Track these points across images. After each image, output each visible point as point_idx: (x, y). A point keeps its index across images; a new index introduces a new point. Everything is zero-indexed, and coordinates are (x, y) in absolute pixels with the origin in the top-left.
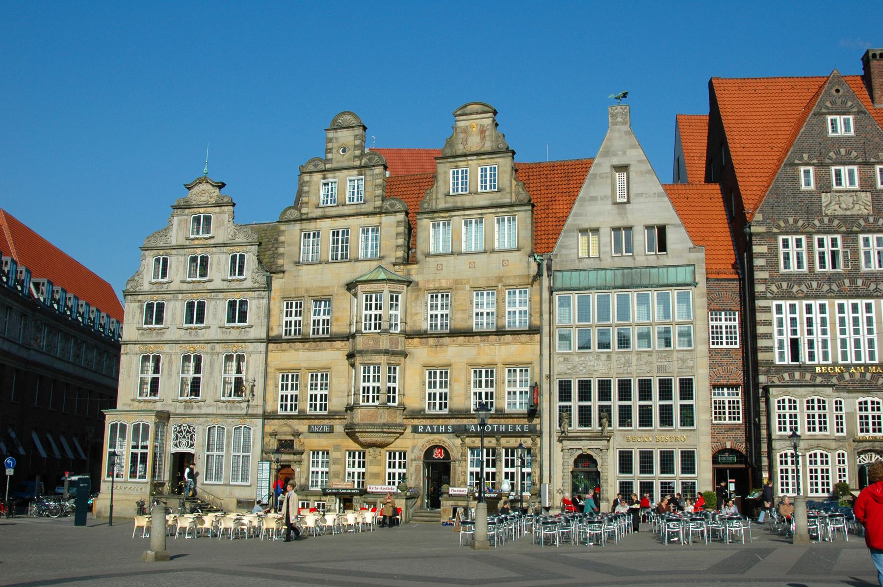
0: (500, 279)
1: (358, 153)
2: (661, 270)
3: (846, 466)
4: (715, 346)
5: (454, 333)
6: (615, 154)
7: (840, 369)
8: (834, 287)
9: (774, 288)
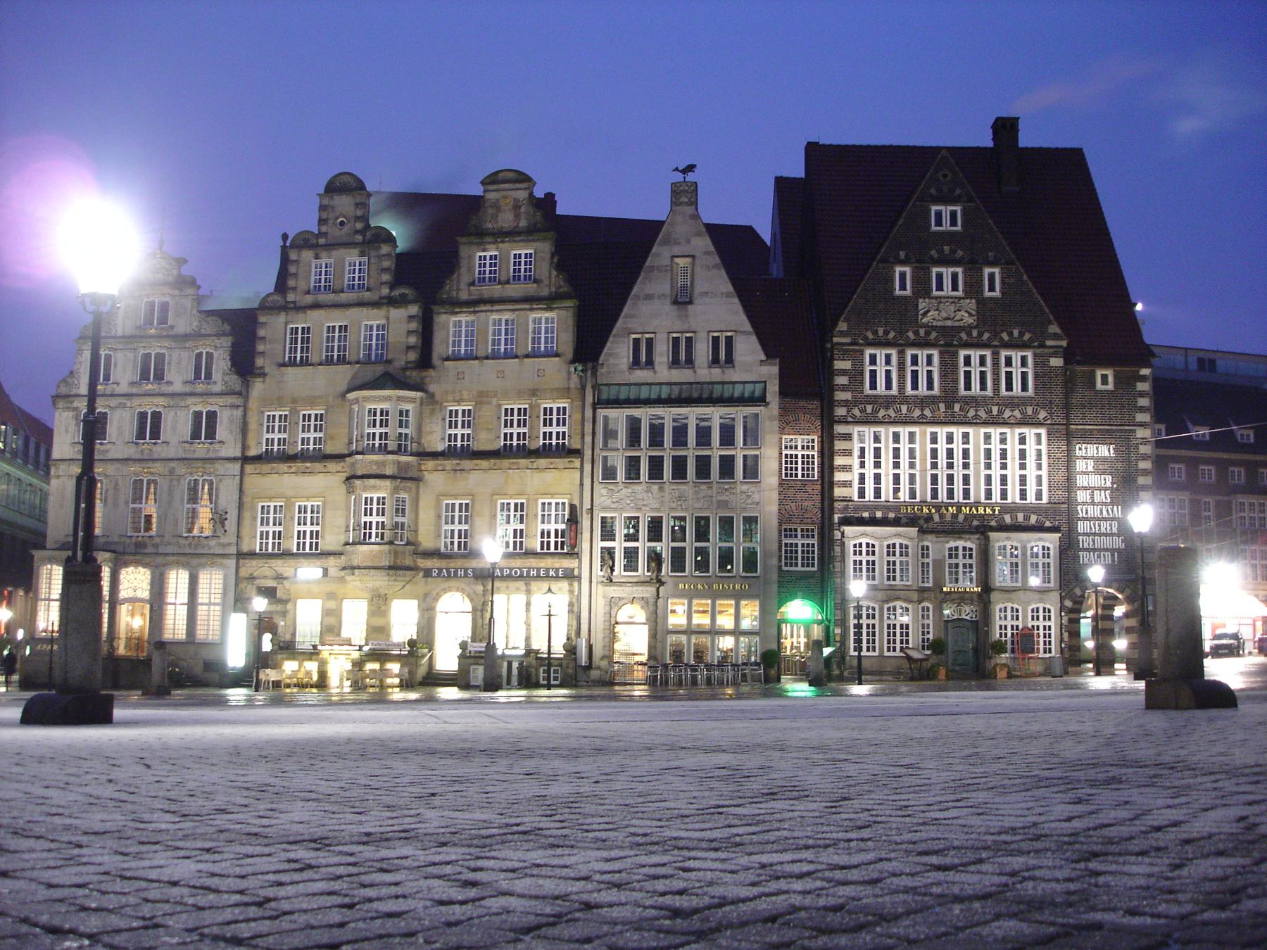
1: (359, 226)
2: (726, 386)
3: (930, 622)
6: (677, 243)
8: (927, 412)
9: (856, 412)
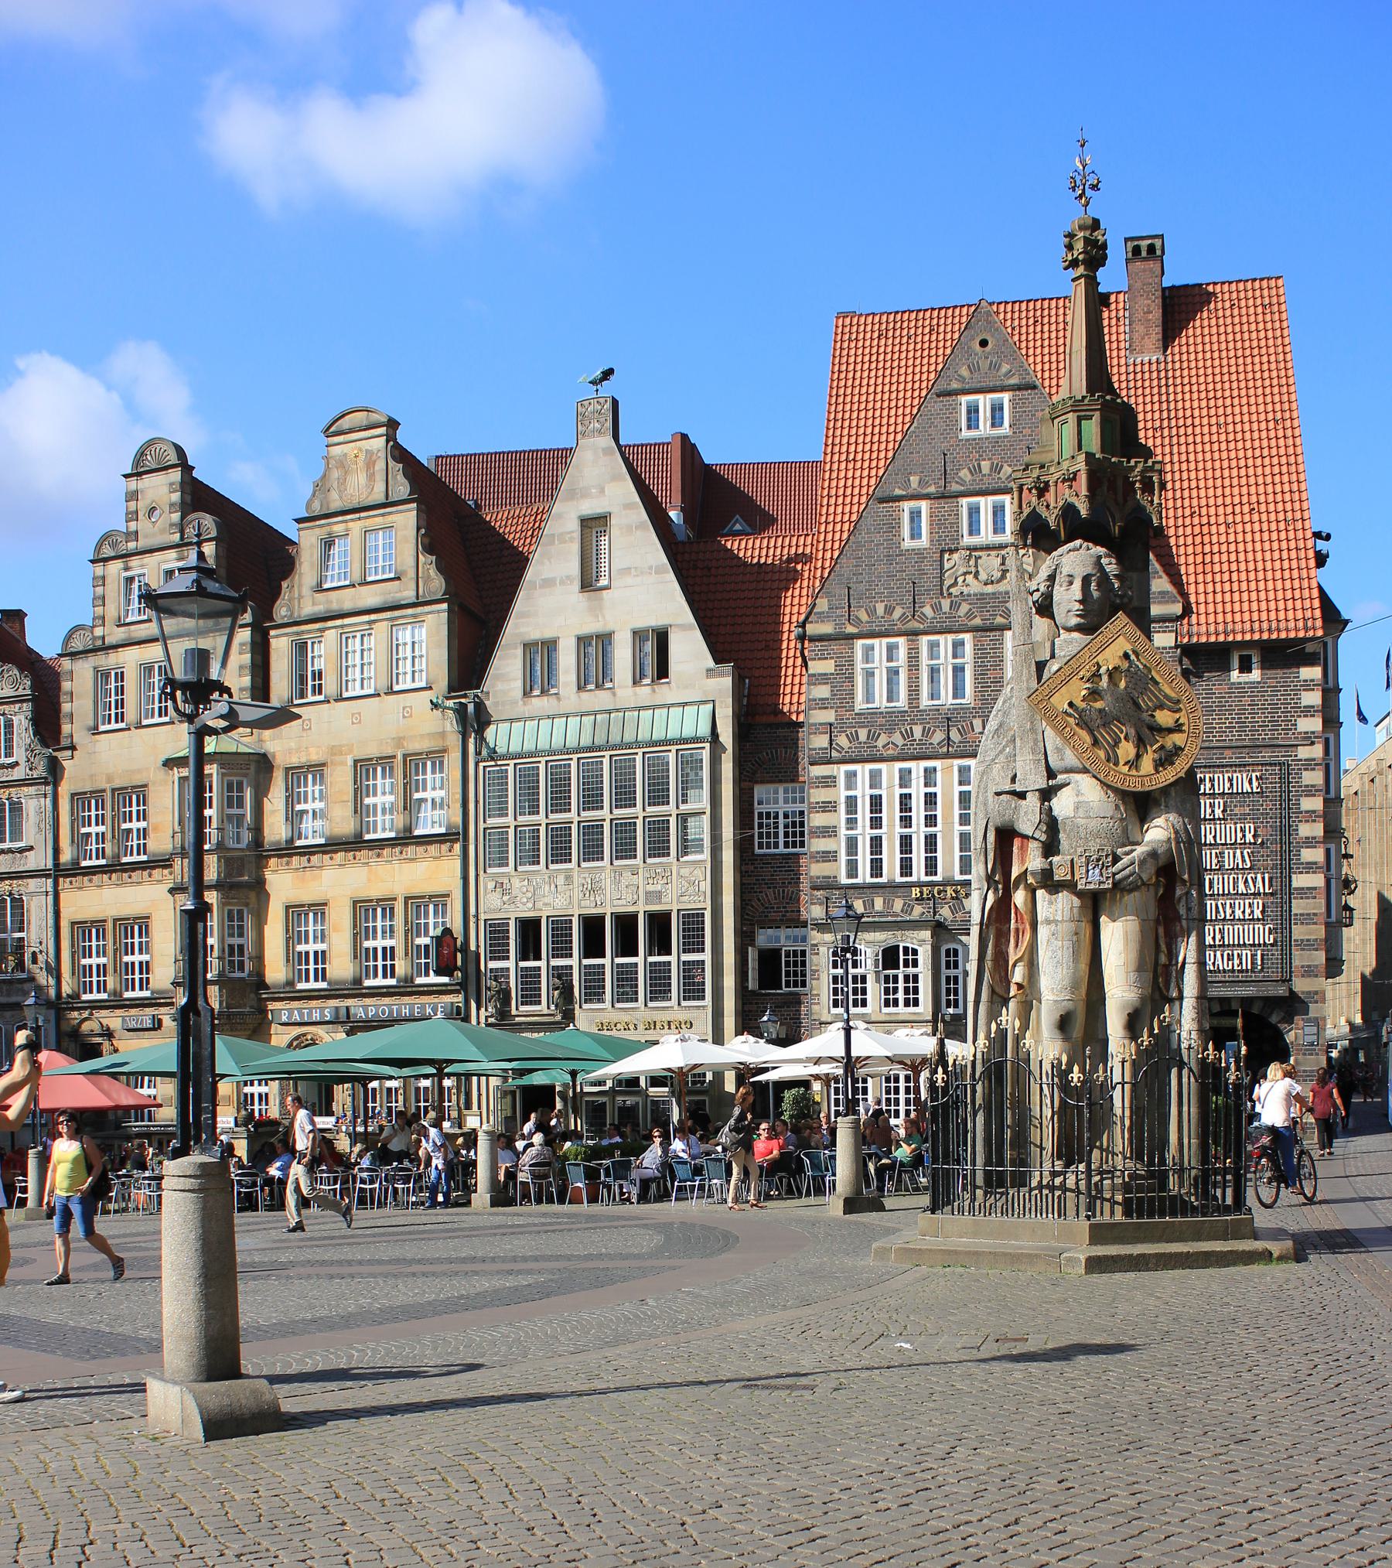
0: (399, 741)
4: (765, 851)
5: (333, 846)
7: (956, 892)
